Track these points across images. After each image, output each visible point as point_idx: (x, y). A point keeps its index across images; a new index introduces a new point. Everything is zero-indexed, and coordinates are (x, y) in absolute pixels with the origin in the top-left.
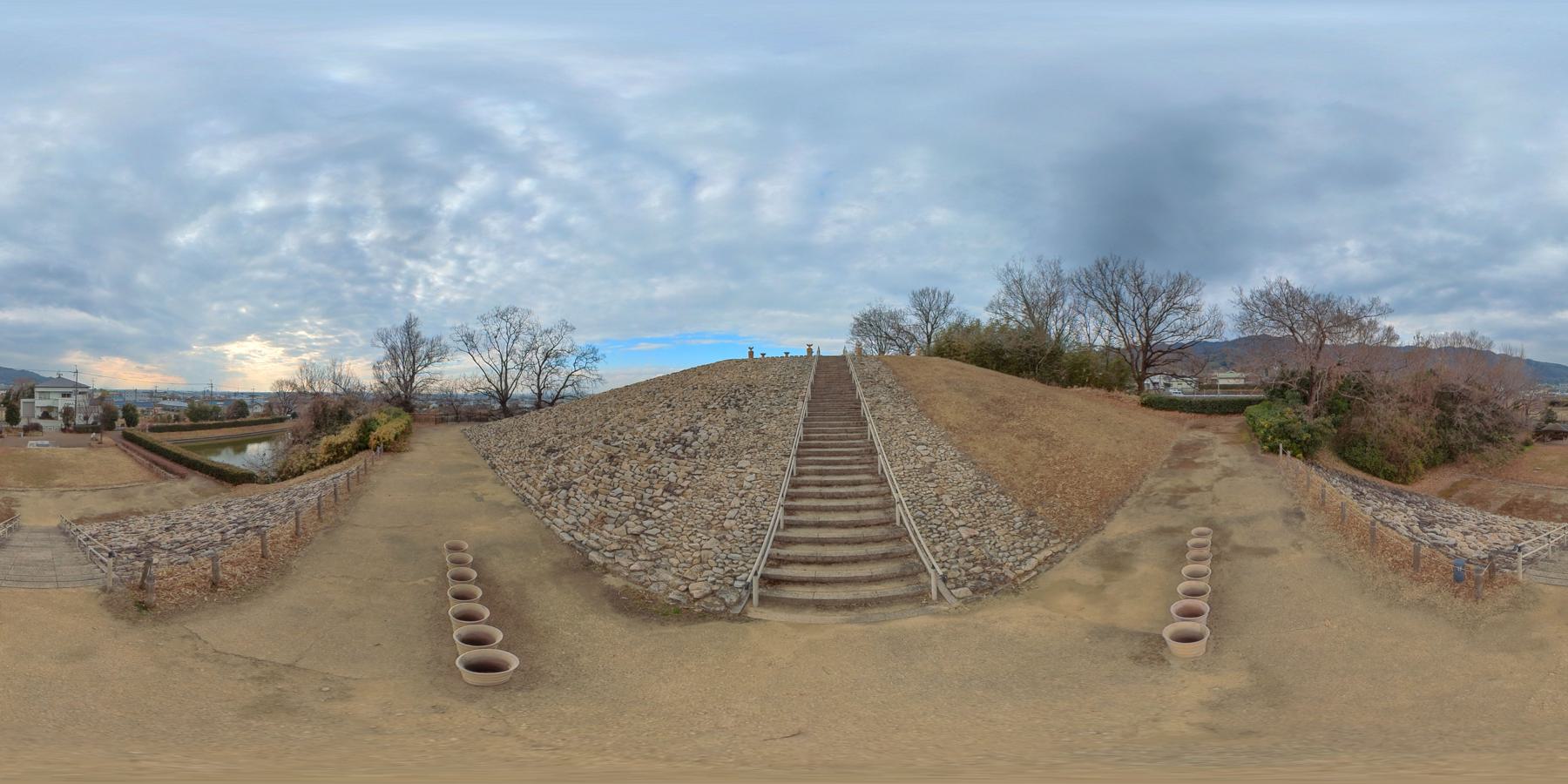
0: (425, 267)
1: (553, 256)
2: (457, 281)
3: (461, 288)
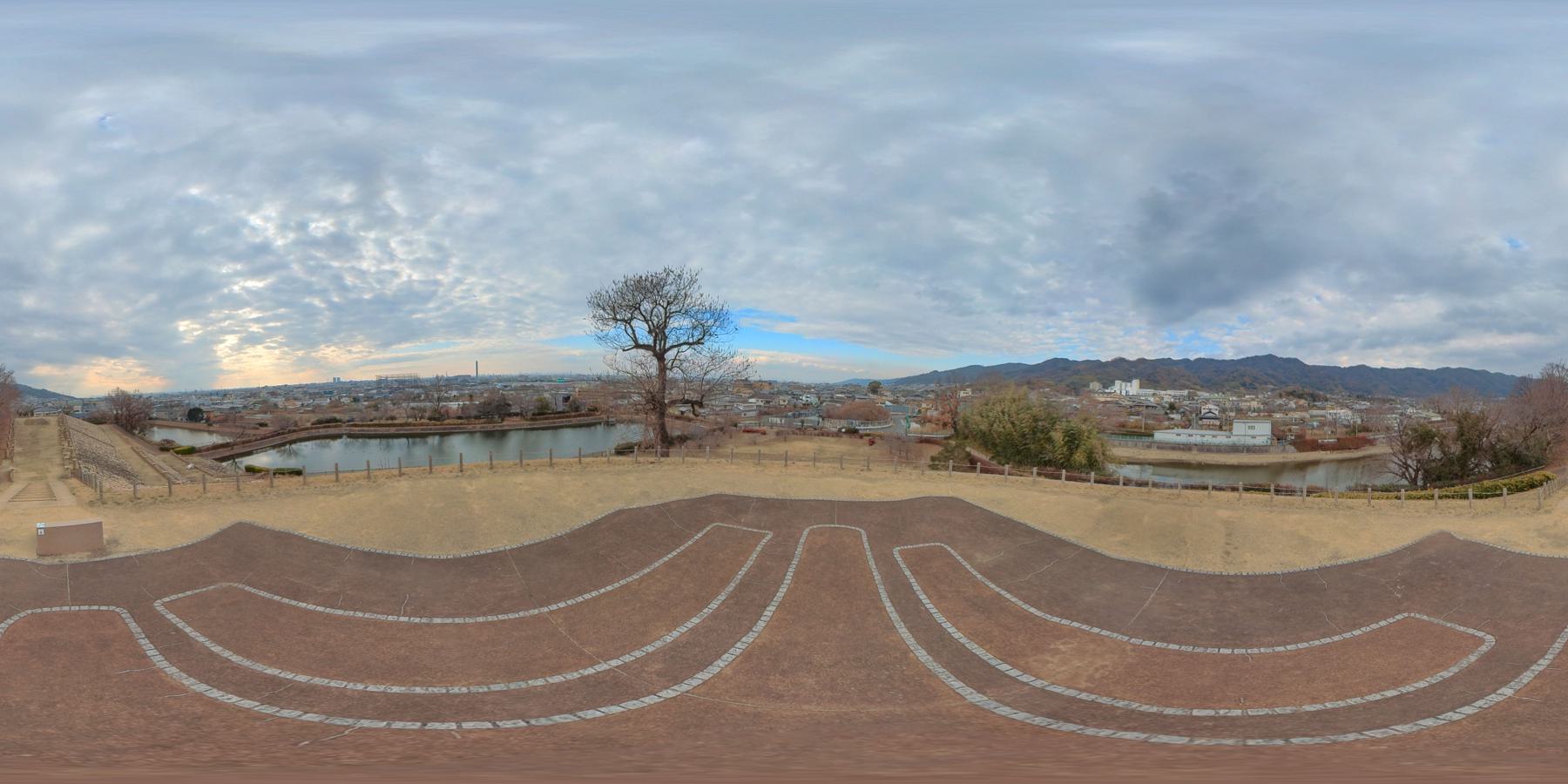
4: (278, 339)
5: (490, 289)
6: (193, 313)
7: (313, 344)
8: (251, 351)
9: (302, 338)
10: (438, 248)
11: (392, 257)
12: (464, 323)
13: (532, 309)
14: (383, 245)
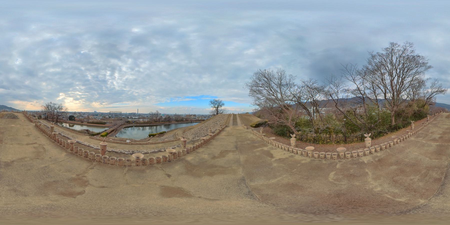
0: (120, 64)
1: (174, 61)
2: (132, 69)
3: (133, 73)
4: (84, 100)
5: (137, 93)
6: (65, 92)
7: (92, 102)
8: (75, 102)
9: (90, 100)
10: (125, 84)
11: (114, 85)
12: (132, 98)
13: (148, 97)
14: (112, 83)
